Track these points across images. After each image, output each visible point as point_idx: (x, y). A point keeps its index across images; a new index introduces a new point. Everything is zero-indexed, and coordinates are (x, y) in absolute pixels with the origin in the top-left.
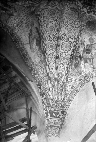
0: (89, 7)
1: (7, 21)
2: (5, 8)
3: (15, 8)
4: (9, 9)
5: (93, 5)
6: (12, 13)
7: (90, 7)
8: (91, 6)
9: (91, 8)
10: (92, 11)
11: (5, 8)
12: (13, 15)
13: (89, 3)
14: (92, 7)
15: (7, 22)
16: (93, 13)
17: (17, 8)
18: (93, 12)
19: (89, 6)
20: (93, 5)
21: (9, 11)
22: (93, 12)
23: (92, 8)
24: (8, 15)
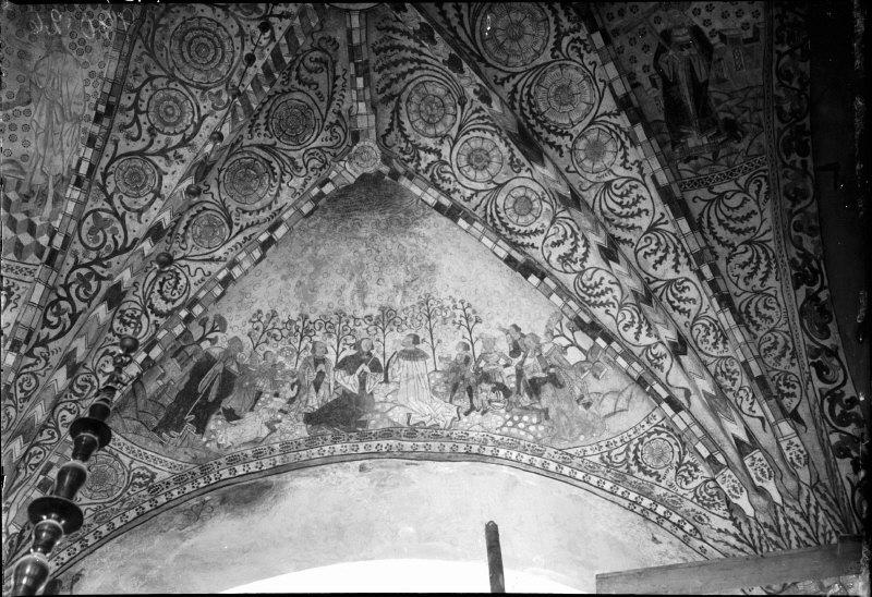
1: (747, 41)
2: (689, 103)
3: (656, 58)
4: (682, 75)
6: (688, 46)
11: (689, 103)
12: (696, 32)
15: (749, 34)
17: (646, 48)
21: (692, 70)
24: (715, 57)
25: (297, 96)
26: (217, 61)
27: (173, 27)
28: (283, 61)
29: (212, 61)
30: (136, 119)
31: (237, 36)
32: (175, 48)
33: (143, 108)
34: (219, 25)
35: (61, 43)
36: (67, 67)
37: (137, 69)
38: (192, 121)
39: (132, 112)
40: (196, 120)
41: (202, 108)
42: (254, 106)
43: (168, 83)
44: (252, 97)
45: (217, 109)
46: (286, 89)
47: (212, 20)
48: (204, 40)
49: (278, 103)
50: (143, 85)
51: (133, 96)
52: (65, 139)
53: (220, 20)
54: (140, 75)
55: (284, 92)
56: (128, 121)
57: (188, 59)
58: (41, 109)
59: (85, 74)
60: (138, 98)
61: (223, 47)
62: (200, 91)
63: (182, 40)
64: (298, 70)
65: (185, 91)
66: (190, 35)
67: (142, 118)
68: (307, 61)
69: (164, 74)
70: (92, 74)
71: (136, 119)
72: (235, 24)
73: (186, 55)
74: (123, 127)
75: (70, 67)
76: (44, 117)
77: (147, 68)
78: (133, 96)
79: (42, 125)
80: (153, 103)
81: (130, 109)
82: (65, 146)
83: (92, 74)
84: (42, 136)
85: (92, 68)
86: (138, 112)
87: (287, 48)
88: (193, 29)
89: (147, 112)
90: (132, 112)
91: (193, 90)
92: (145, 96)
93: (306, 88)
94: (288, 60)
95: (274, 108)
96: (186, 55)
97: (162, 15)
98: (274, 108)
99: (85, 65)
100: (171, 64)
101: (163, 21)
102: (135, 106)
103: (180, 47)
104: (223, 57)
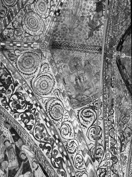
0: (3, 89)
5: (9, 89)
7: (5, 89)
8: (6, 89)
9: (4, 90)
10: (3, 96)
13: (6, 83)
14: (7, 90)
16: (3, 99)
18: (3, 98)
19: (3, 87)
20: (9, 89)
22: (3, 99)
23: (5, 92)
25: (8, 4)
26: (29, 18)
27: (39, 30)
28: (8, 18)
29: (30, 19)
30: (51, 7)
31: (23, 25)
32: (39, 25)
33: (48, 10)
34: (28, 28)
35: (70, 31)
36: (69, 24)
37: (48, 22)
38: (36, 2)
39: (51, 9)
40: (35, 3)
41: (33, 6)
42: (16, 5)
43: (42, 16)
44: (17, 8)
45: (29, 5)
46: (10, 7)
47: (30, 30)
48: (32, 25)
49: (13, 3)
50: (48, 17)
51: (50, 15)
52: (73, 4)
53: (28, 30)
54: (48, 20)
55: (11, 6)
56: (53, 7)
57: (36, 21)
58: (78, 14)
59: (64, 22)
60: (49, 14)
61: (27, 22)
62: (34, 11)
63: (37, 26)
64: (7, 12)
65: (38, 12)
66: (35, 27)
67: (49, 7)
68: (4, 15)
69: (43, 19)
70: (62, 22)
71: (51, 7)
72: (24, 28)
73: (37, 22)
74: (54, 5)
75: (68, 25)
76: (78, 11)
77: (46, 21)
78: (50, 15)
79: (79, 9)
80: (46, 10)
81: (52, 11)
82: (73, 2)
83: (62, 22)
84: (80, 6)
85: (62, 23)
86: (50, 9)
87: (7, 21)
88: (35, 28)
89: (48, 9)
90: (51, 9)
91: (35, 12)
92: (47, 13)
93: (6, 6)
94: (6, 18)
95: (14, 2)
96: (37, 22)
97: (41, 34)
98: (14, 2)
99: (64, 24)
100: (40, 21)
101: (41, 32)
102: (50, 11)
103: (38, 25)
104: (27, 19)
